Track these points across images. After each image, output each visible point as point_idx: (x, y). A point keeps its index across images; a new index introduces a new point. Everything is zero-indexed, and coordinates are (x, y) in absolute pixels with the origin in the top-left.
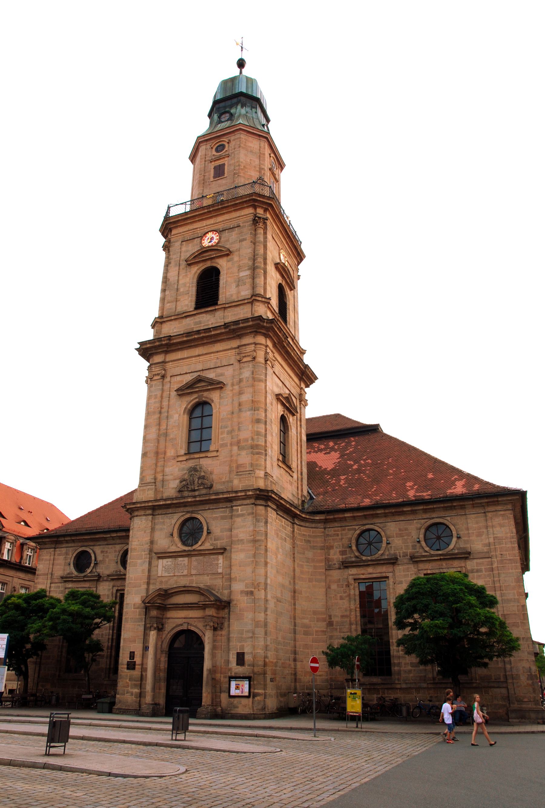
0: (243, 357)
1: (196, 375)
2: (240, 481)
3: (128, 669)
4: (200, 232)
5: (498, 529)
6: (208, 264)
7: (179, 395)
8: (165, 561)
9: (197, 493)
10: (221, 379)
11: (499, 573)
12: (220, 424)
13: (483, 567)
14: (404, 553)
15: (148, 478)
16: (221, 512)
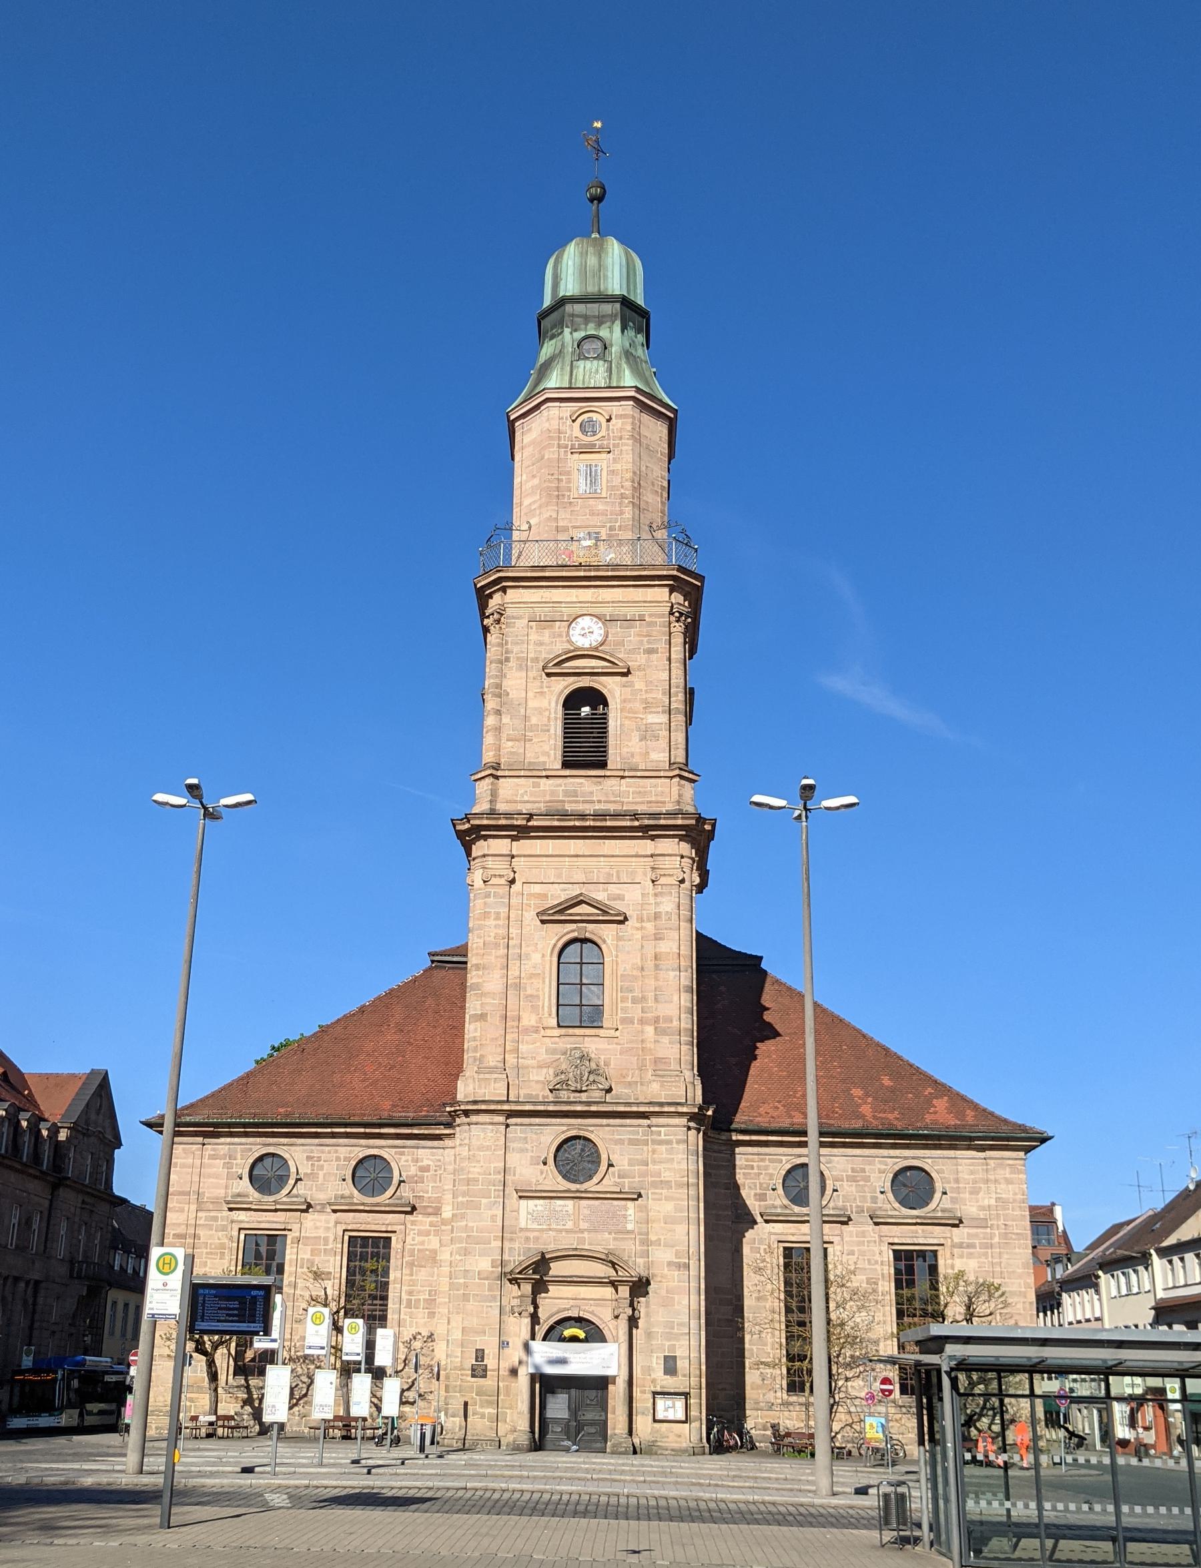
1: (574, 891)
2: (662, 1086)
4: (567, 612)
5: (1003, 1186)
6: (585, 682)
7: (543, 922)
8: (531, 1203)
9: (584, 1097)
10: (619, 906)
11: (1000, 1253)
13: (977, 1241)
14: (857, 1207)
15: (491, 1060)
16: (629, 1132)
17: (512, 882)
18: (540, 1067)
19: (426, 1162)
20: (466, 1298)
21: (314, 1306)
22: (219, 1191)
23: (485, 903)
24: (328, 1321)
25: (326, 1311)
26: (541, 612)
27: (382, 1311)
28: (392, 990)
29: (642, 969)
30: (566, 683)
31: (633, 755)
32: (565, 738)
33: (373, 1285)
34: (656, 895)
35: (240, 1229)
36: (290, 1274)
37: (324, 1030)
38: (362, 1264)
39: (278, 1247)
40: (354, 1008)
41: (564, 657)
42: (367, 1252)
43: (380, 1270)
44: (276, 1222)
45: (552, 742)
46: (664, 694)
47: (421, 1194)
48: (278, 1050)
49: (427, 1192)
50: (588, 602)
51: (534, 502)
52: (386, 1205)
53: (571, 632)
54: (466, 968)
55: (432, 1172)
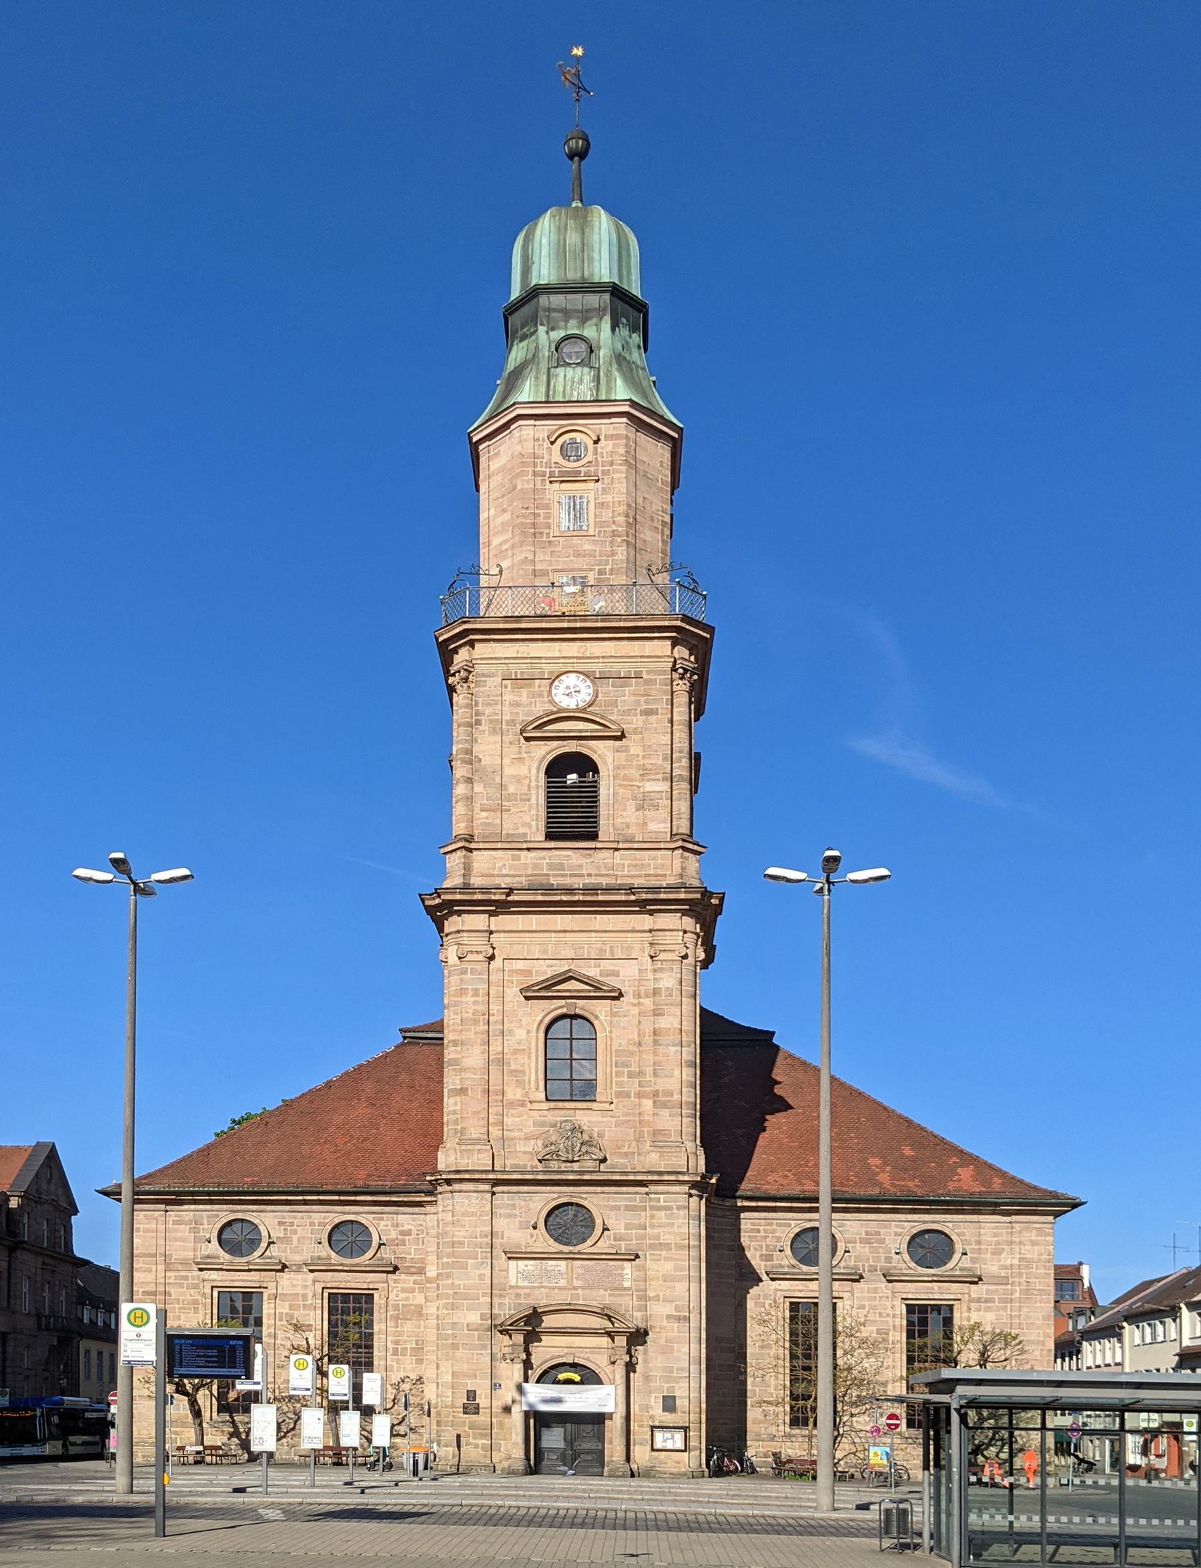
0: (660, 951)
1: (563, 967)
3: (465, 1413)
6: (571, 747)
8: (521, 1263)
9: (576, 1166)
12: (614, 1059)
15: (473, 1132)
17: (492, 958)
18: (527, 1138)
19: (406, 1227)
20: (455, 1346)
21: (296, 1354)
22: (187, 1253)
23: (461, 980)
24: (311, 1367)
25: (309, 1358)
26: (516, 669)
27: (368, 1358)
28: (361, 1066)
29: (640, 1044)
30: (548, 748)
31: (628, 826)
32: (548, 807)
33: (357, 1336)
34: (655, 971)
35: (213, 1287)
36: (269, 1326)
37: (288, 1104)
38: (344, 1317)
39: (254, 1302)
40: (320, 1082)
41: (545, 719)
42: (349, 1307)
43: (363, 1322)
44: (251, 1281)
45: (534, 812)
46: (665, 759)
47: (403, 1255)
48: (239, 1123)
49: (410, 1254)
50: (574, 658)
51: (506, 541)
52: (366, 1266)
53: (554, 691)
54: (443, 1044)
55: (414, 1236)
